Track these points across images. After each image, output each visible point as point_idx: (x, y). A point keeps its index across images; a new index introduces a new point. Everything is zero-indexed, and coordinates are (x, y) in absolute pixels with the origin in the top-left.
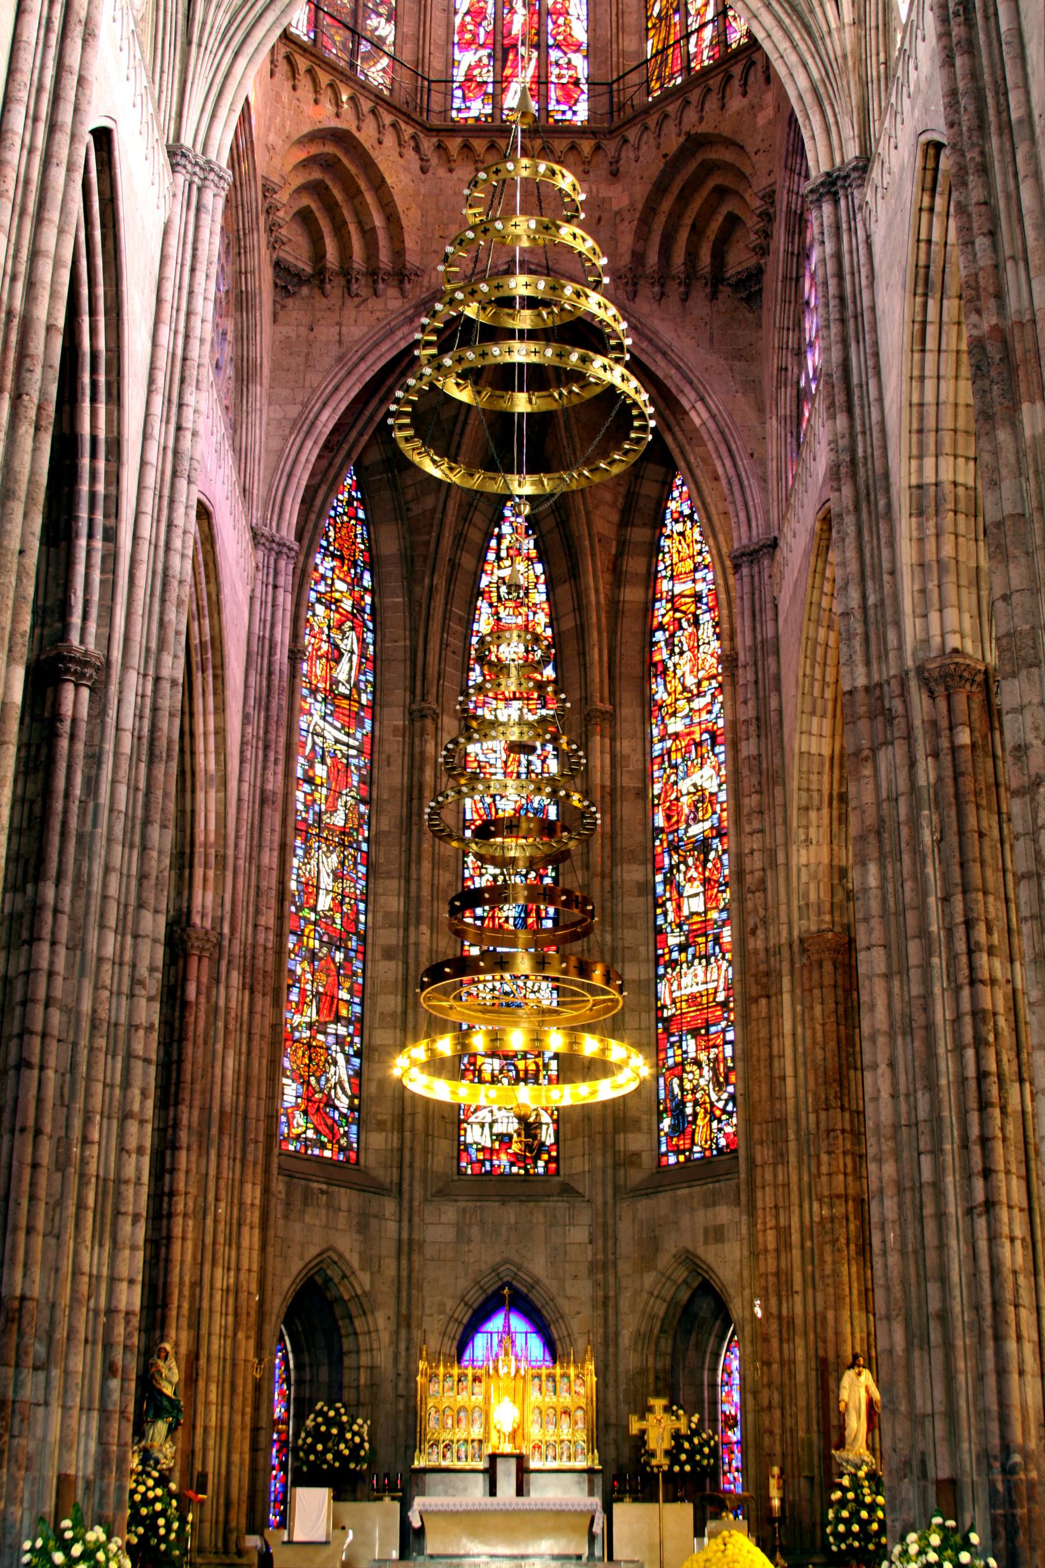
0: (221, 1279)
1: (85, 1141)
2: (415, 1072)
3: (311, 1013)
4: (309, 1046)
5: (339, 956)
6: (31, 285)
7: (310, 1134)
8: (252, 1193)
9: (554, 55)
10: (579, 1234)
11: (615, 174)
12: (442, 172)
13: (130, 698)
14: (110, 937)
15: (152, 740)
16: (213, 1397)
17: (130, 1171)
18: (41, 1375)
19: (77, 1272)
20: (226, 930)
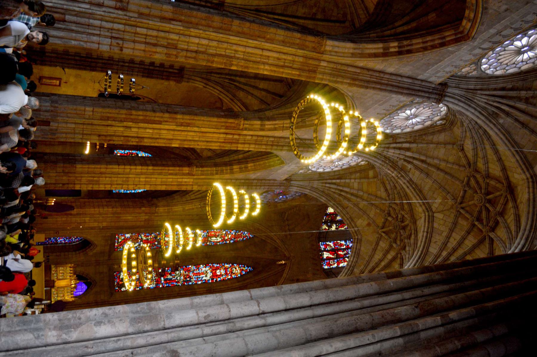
0: (87, 219)
1: (106, 177)
2: (128, 246)
3: (144, 238)
4: (138, 238)
5: (156, 243)
6: (244, 143)
7: (120, 240)
8: (105, 224)
9: (336, 260)
10: (102, 297)
13: (188, 180)
14: (144, 179)
15: (181, 185)
16: (63, 219)
17: (101, 186)
18: (61, 171)
19: (81, 177)
20: (156, 215)
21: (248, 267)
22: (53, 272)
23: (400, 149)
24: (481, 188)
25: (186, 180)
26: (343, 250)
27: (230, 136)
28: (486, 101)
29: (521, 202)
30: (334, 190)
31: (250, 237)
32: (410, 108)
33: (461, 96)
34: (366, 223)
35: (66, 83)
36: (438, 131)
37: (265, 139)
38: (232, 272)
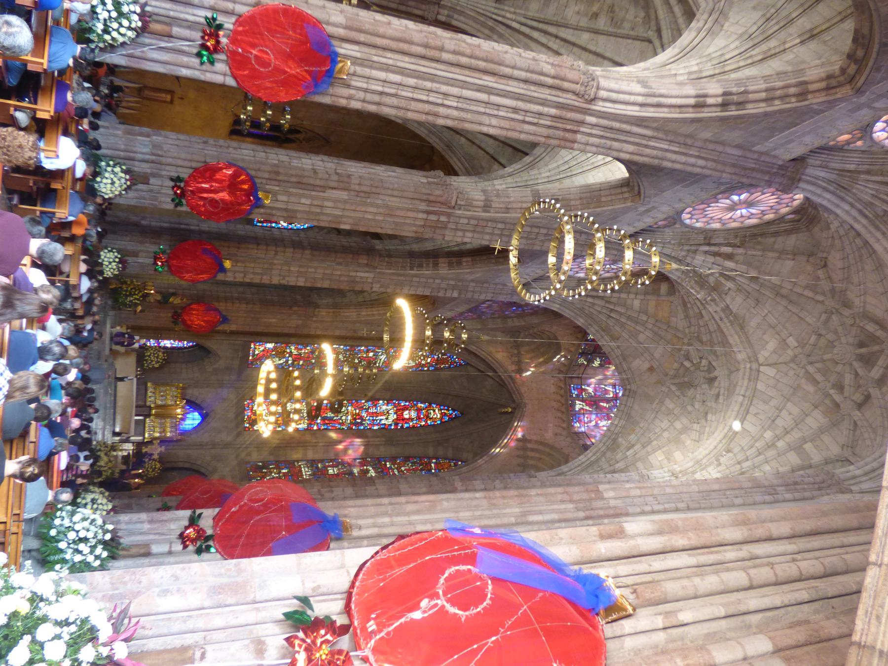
7: (257, 352)
11: (556, 434)
12: (552, 381)
13: (366, 275)
21: (454, 410)
22: (149, 394)
23: (716, 254)
25: (362, 274)
26: (608, 401)
27: (433, 217)
28: (874, 192)
30: (599, 309)
31: (461, 365)
32: (739, 192)
33: (830, 182)
34: (647, 365)
35: (182, 98)
36: (786, 231)
37: (490, 224)
38: (427, 417)
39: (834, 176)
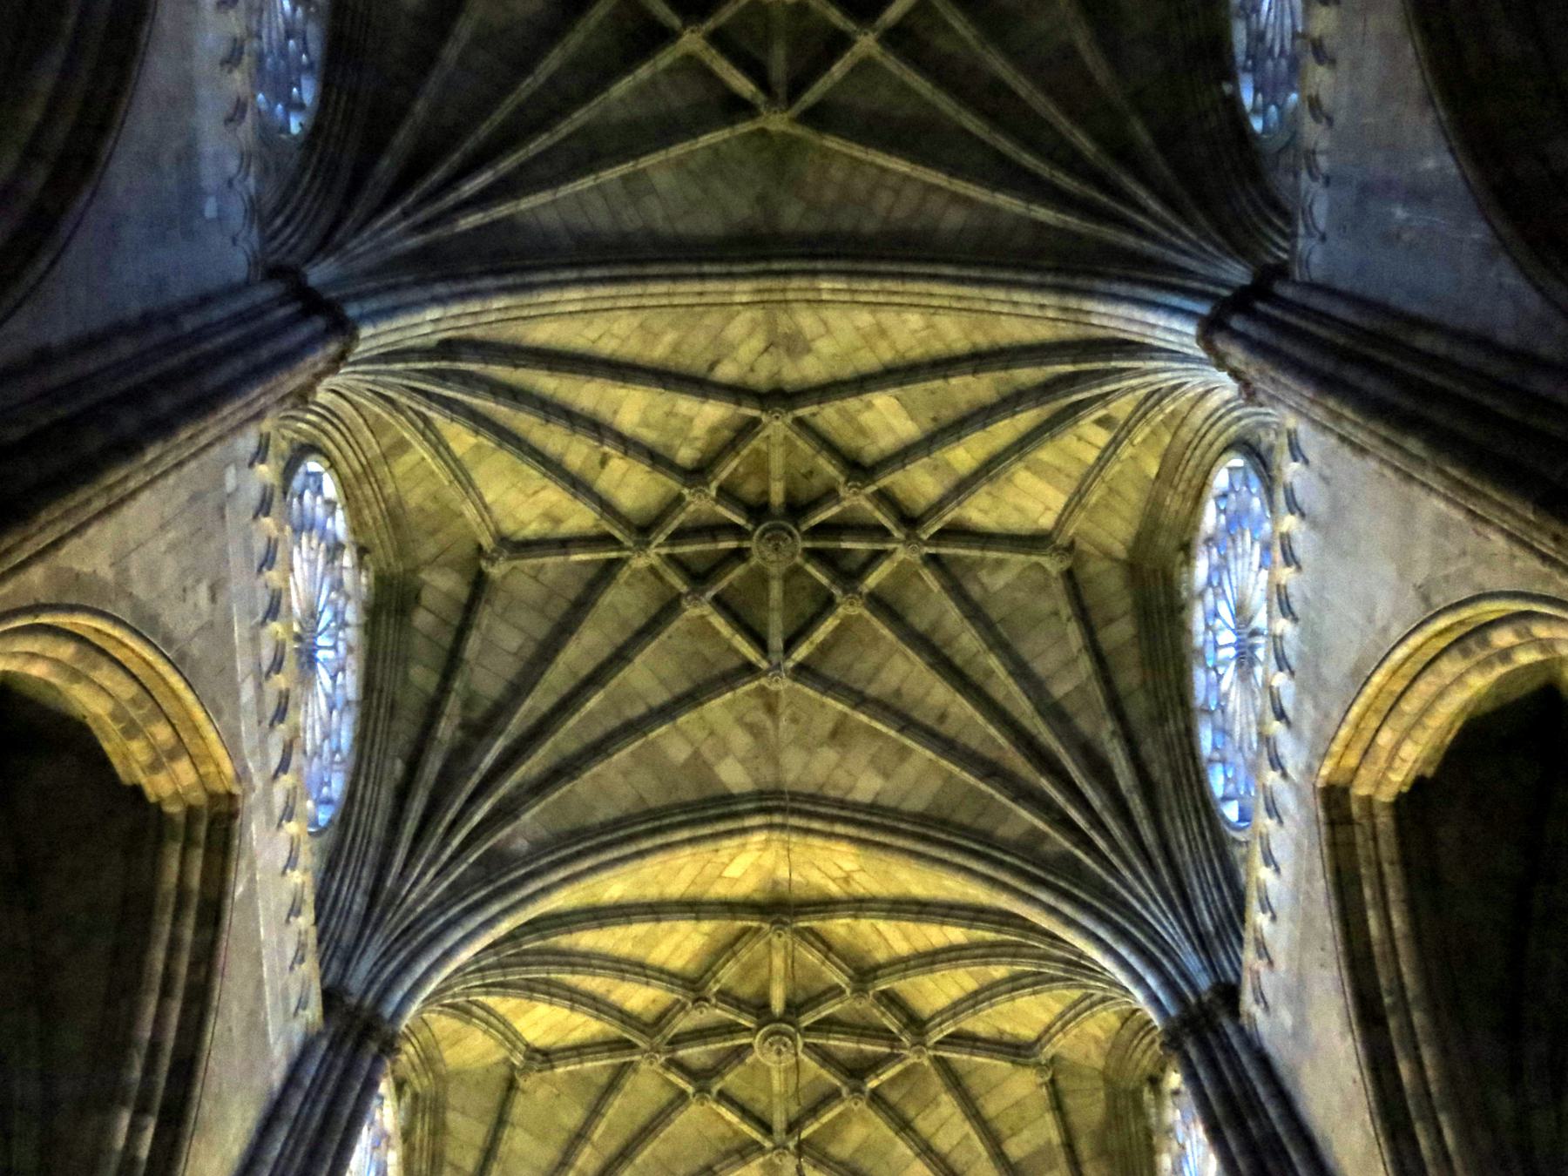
24: (731, 1029)
28: (432, 871)
29: (847, 879)
33: (387, 955)
39: (378, 939)
